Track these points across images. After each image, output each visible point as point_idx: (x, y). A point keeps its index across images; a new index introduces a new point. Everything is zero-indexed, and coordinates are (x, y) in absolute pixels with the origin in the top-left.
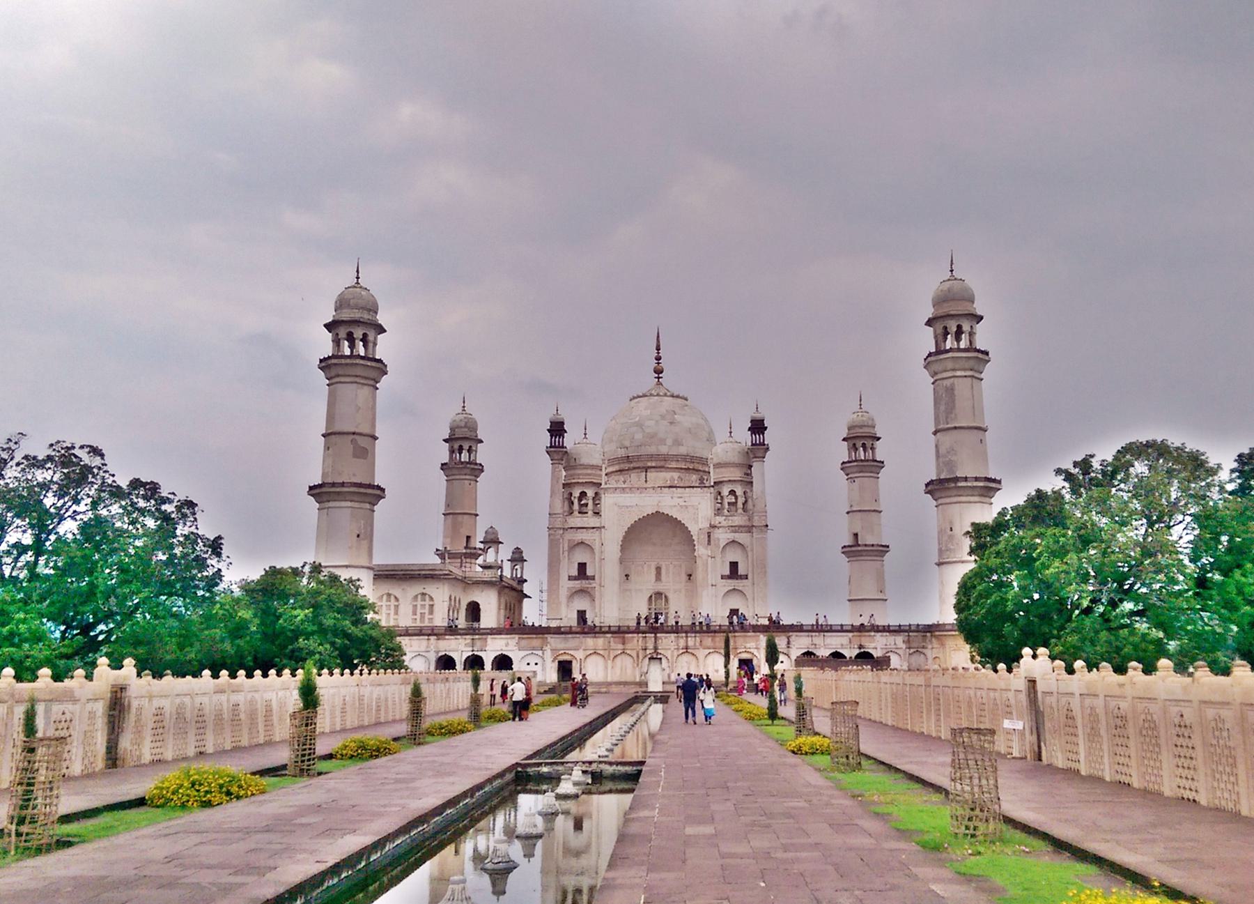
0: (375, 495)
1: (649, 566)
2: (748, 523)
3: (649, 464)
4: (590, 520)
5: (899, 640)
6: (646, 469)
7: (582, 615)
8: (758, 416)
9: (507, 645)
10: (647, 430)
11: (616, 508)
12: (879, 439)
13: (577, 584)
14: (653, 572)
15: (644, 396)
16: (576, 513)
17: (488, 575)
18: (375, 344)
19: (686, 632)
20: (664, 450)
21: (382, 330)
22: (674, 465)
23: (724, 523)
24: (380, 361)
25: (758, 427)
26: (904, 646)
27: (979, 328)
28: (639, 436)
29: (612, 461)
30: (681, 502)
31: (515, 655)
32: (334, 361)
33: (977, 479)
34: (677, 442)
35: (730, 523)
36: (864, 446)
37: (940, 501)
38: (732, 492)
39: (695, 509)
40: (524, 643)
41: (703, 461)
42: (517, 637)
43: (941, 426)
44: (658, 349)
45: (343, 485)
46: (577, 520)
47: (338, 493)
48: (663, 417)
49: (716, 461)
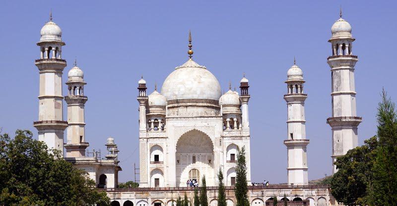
0: (64, 126)
1: (189, 156)
2: (240, 135)
3: (188, 104)
4: (159, 134)
5: (314, 192)
6: (187, 106)
7: (157, 180)
8: (244, 80)
9: (130, 196)
10: (187, 87)
11: (173, 128)
12: (304, 82)
13: (155, 166)
14: (191, 158)
15: (185, 67)
16: (152, 130)
17: (111, 162)
18: (61, 51)
19: (215, 190)
20: (196, 97)
21: (64, 44)
22: (201, 104)
23: (228, 135)
24: (64, 61)
25: (244, 87)
26: (316, 195)
27: (353, 43)
28: (182, 90)
29: (170, 102)
30: (206, 124)
31: (134, 201)
32: (44, 62)
33: (350, 118)
34: (202, 93)
35: (231, 135)
36: (296, 86)
37: (335, 127)
38: (232, 119)
39: (213, 128)
40: (138, 195)
41: (216, 102)
42: (135, 192)
43: (335, 92)
44: (190, 42)
45: (51, 122)
46: (153, 133)
47: (49, 126)
48: (195, 80)
49: (223, 104)
